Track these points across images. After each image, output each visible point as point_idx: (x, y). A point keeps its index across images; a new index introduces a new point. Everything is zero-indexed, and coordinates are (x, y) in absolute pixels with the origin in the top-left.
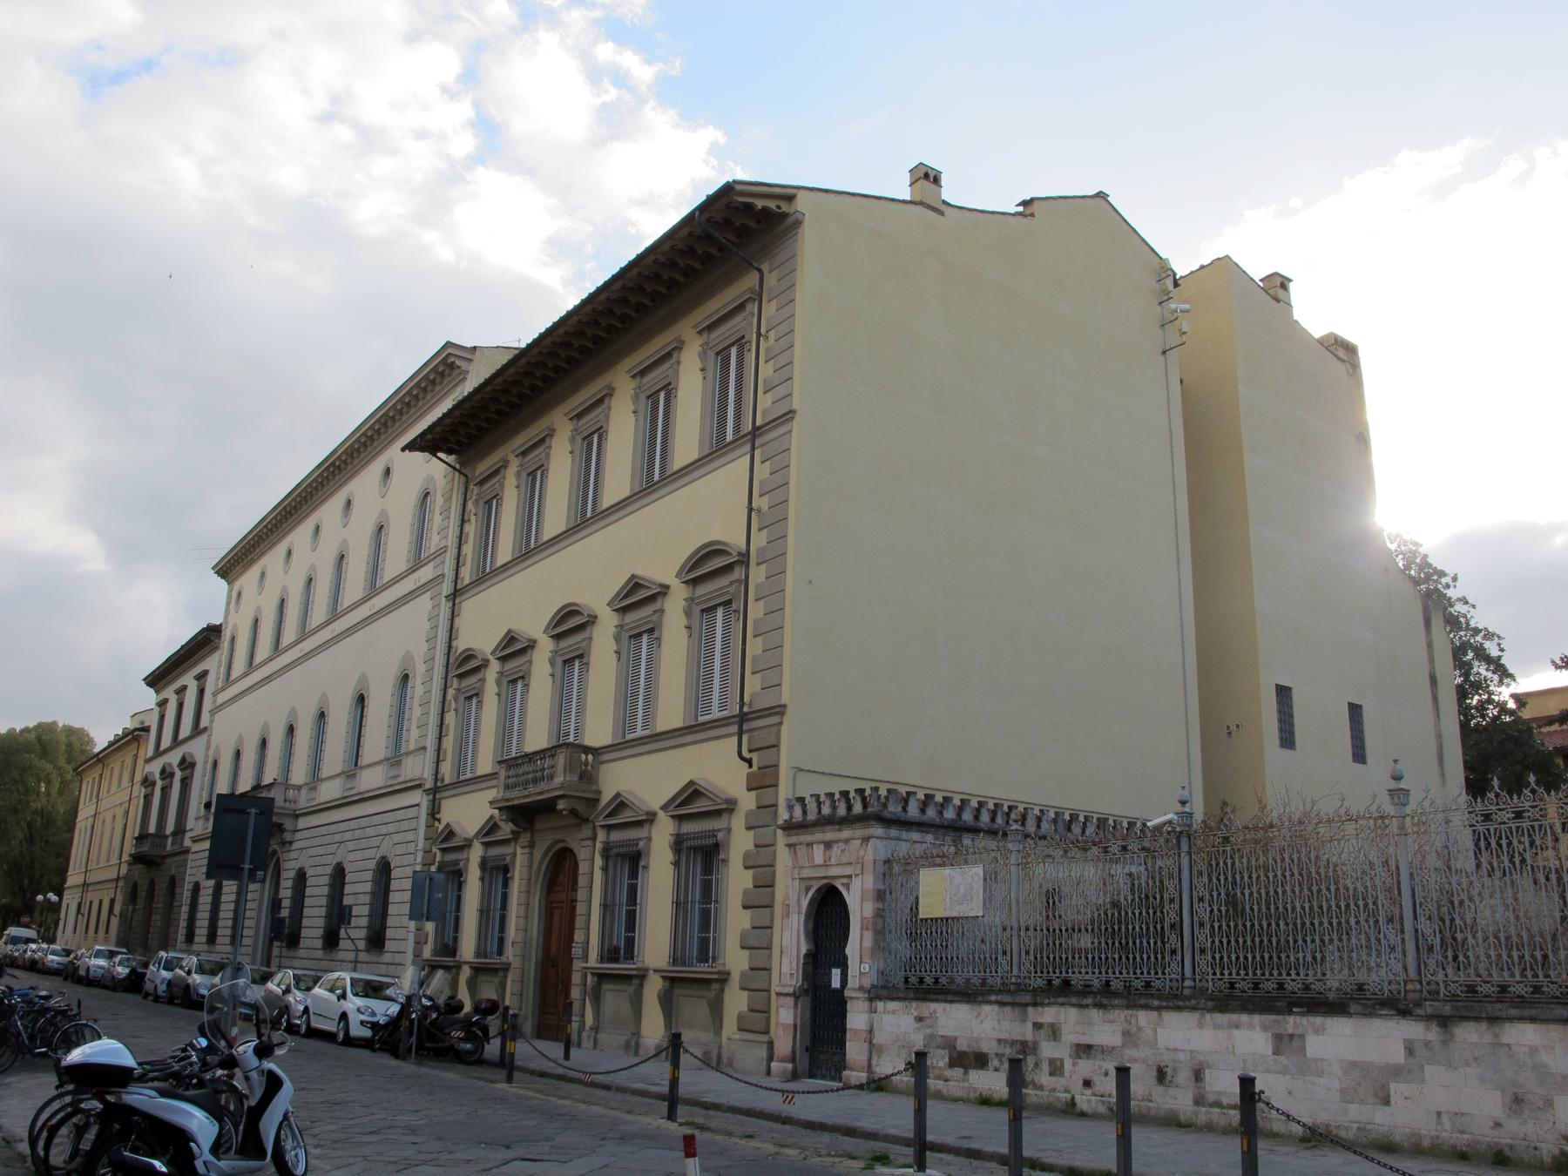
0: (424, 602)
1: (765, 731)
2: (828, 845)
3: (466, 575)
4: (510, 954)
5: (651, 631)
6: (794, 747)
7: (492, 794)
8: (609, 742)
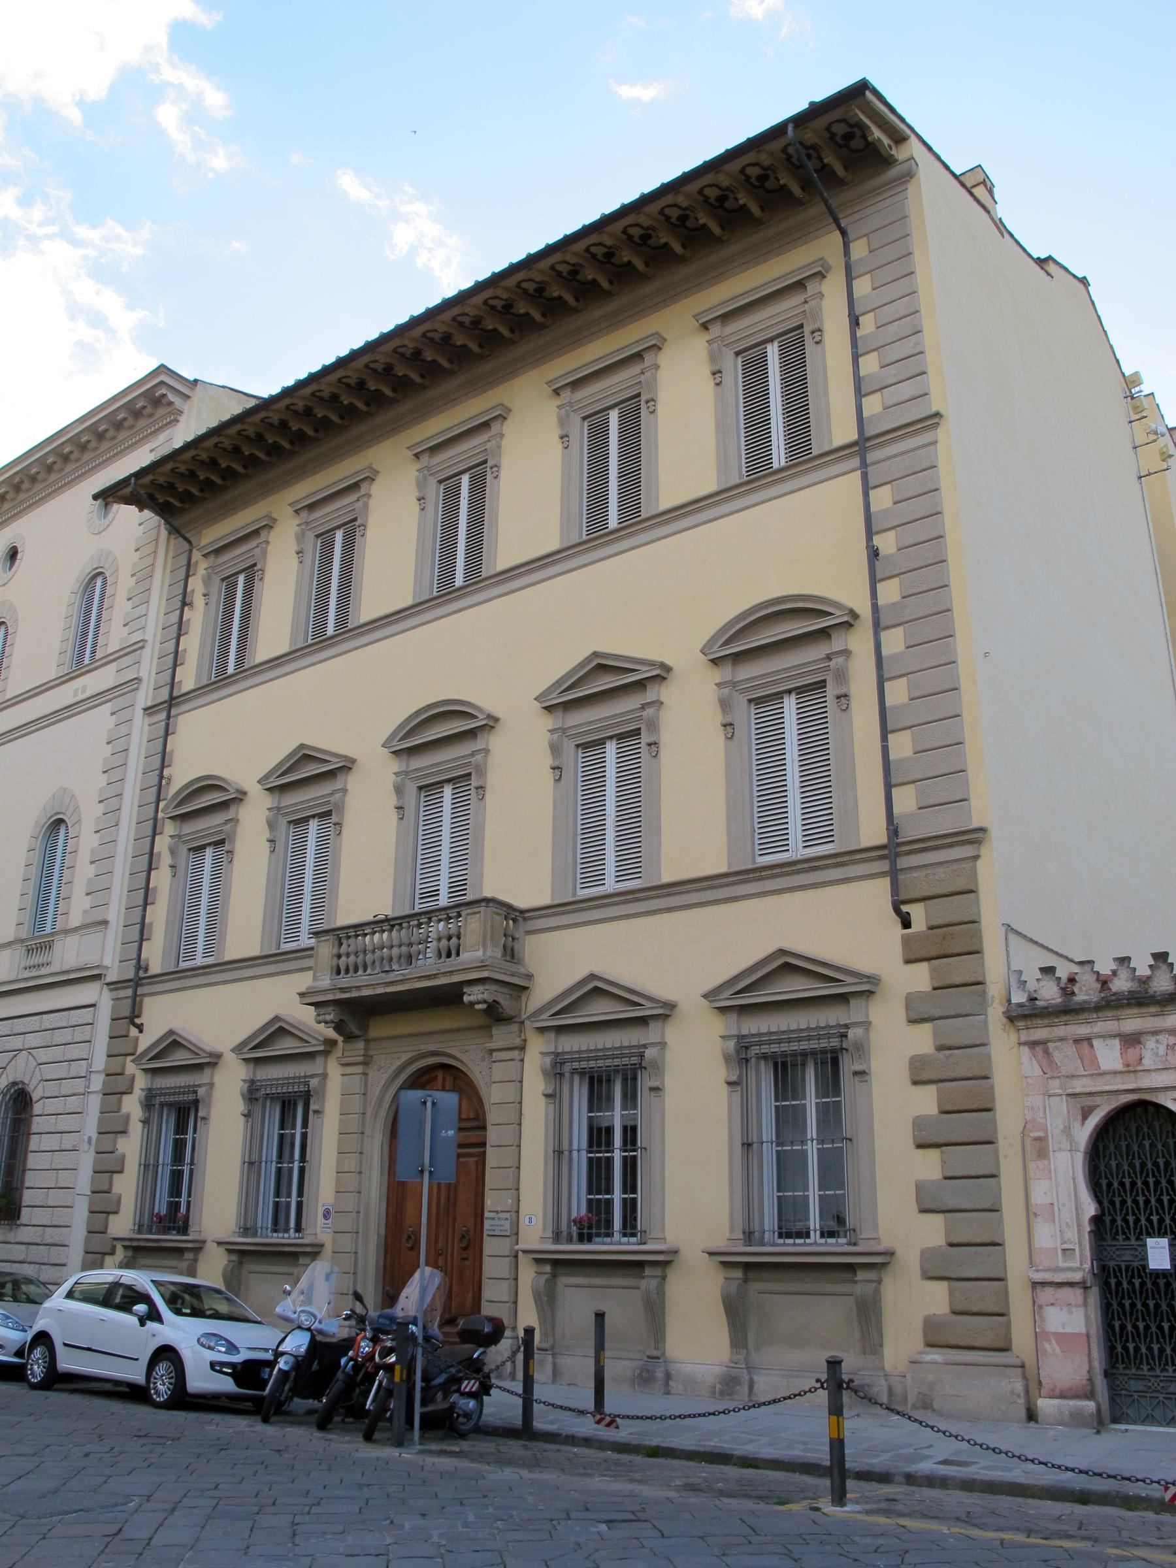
0: (101, 719)
1: (940, 870)
2: (1131, 1040)
3: (188, 678)
4: (318, 1229)
5: (328, 814)
6: (1004, 892)
7: (304, 981)
8: (546, 900)
